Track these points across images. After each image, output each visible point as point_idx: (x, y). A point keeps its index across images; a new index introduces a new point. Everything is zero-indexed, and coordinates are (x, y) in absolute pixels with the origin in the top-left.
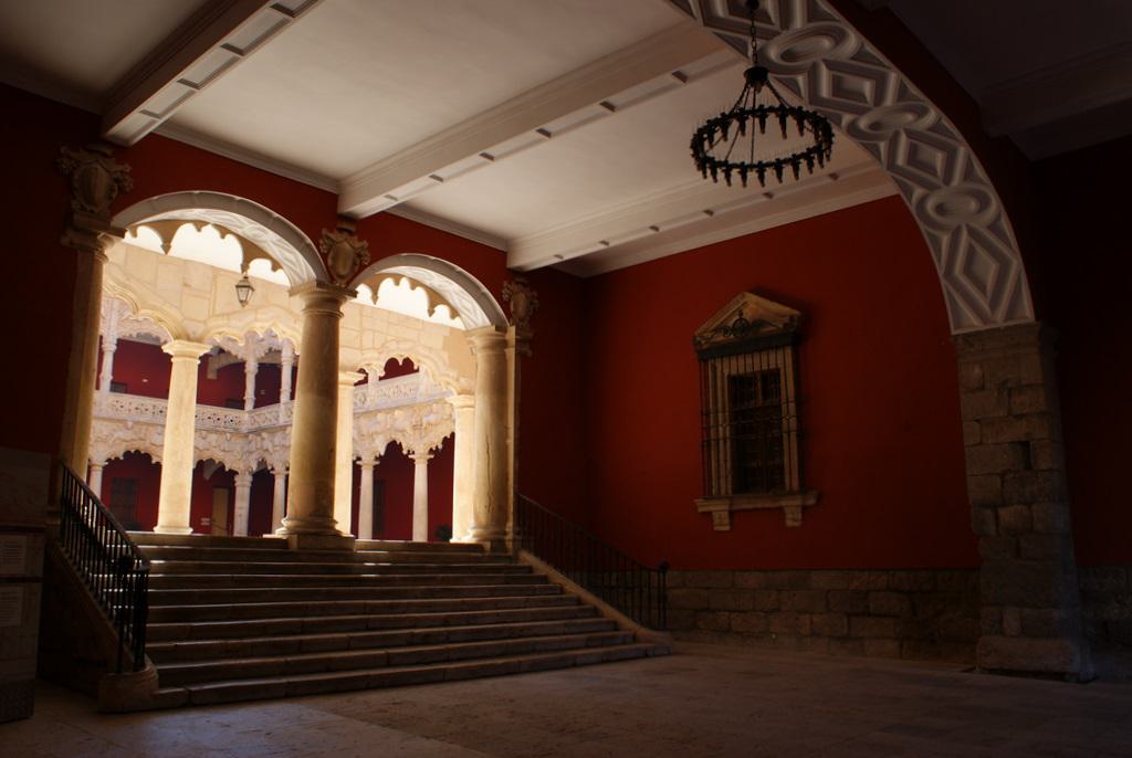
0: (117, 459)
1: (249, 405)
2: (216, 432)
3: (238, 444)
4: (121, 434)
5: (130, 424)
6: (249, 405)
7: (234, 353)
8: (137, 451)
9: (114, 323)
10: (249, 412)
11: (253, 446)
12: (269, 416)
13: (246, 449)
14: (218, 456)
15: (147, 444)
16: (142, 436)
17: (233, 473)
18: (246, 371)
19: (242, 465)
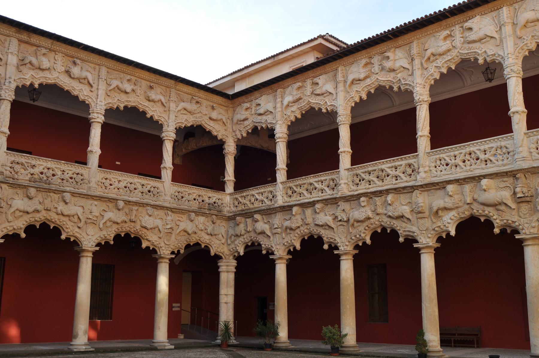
0: (107, 243)
1: (230, 188)
2: (203, 214)
3: (222, 228)
4: (110, 215)
5: (121, 204)
6: (230, 188)
7: (215, 133)
8: (127, 235)
9: (101, 92)
10: (230, 194)
11: (241, 228)
12: (260, 197)
13: (231, 232)
14: (205, 239)
15: (138, 227)
16: (133, 218)
17: (217, 257)
18: (226, 151)
19: (225, 245)
